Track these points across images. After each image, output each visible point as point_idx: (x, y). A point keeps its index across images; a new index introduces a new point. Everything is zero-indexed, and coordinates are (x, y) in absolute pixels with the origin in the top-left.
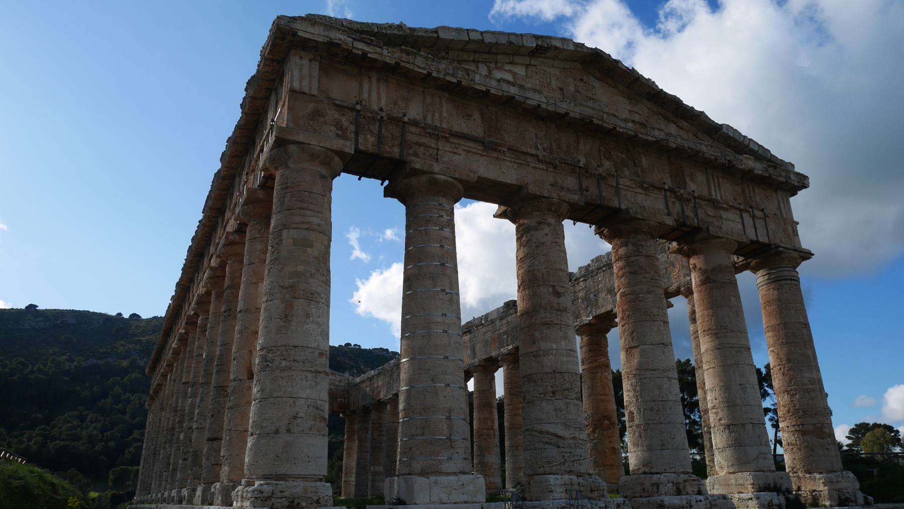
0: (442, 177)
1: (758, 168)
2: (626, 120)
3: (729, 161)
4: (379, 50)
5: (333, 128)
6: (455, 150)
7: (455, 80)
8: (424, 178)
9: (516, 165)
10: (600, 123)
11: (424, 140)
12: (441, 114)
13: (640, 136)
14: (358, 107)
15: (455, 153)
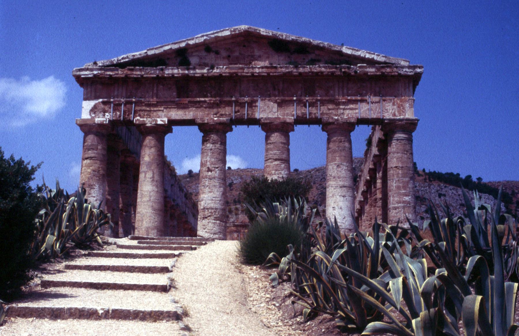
0: (149, 125)
1: (371, 70)
2: (262, 68)
3: (344, 72)
4: (117, 72)
5: (102, 113)
6: (160, 109)
7: (155, 76)
8: (142, 126)
9: (194, 109)
10: (243, 74)
11: (144, 108)
12: (153, 92)
13: (271, 74)
14: (112, 100)
15: (160, 110)
